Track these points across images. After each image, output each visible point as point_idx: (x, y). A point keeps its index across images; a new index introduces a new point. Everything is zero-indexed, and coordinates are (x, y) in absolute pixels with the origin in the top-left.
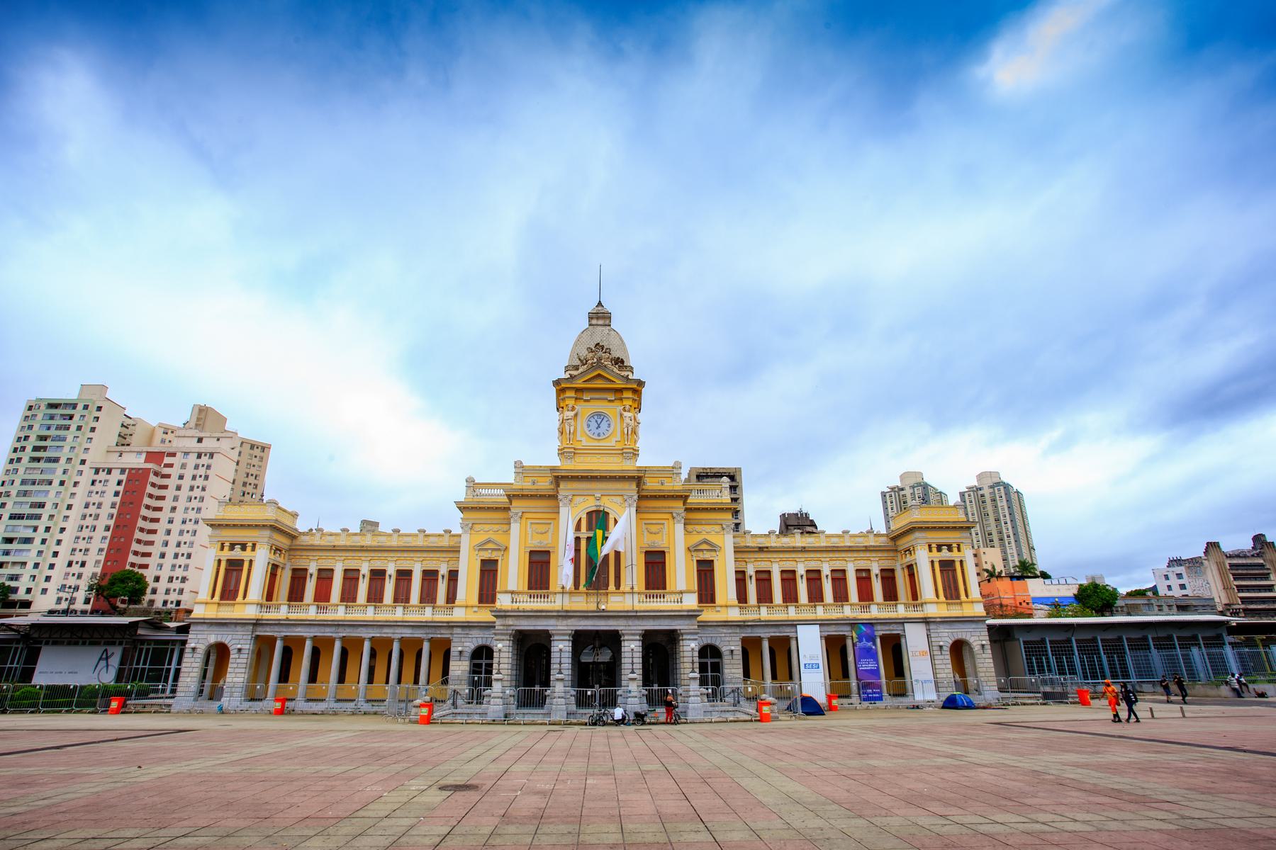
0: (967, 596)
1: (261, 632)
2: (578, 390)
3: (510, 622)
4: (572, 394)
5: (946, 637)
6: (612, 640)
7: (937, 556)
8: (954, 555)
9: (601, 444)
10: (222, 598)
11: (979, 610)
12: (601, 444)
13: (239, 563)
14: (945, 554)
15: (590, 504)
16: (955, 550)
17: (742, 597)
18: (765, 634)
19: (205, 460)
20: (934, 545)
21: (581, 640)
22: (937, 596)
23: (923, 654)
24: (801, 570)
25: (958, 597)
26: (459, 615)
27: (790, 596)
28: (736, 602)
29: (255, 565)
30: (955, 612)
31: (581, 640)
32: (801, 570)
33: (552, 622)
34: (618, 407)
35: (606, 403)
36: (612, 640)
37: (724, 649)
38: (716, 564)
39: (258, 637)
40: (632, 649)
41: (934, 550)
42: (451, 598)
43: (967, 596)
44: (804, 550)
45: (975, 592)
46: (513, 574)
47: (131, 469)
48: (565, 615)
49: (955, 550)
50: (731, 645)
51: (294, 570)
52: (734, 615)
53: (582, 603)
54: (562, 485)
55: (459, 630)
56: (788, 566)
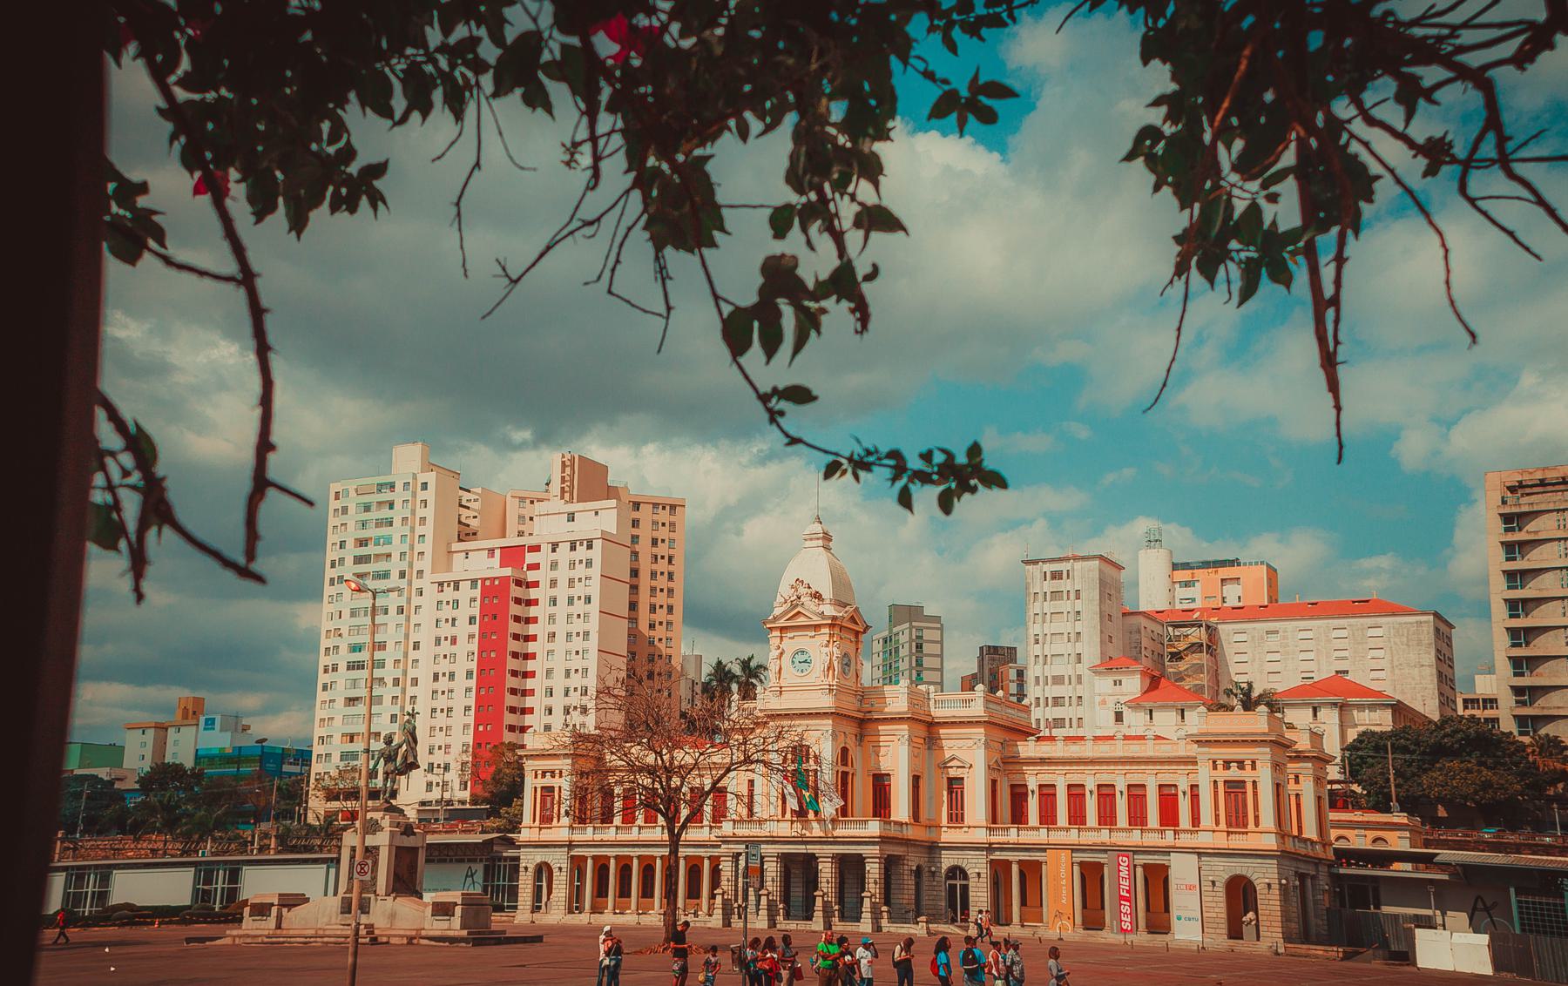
0: (1257, 824)
2: (782, 629)
5: (1223, 870)
7: (1222, 775)
8: (1247, 775)
9: (804, 680)
11: (1270, 842)
12: (804, 680)
13: (551, 789)
14: (1234, 773)
16: (1248, 768)
19: (581, 553)
20: (1220, 762)
21: (786, 860)
22: (1217, 823)
23: (1191, 888)
24: (1090, 785)
30: (1238, 842)
31: (786, 860)
32: (1090, 785)
37: (971, 872)
41: (1220, 767)
43: (1257, 824)
44: (1093, 762)
47: (484, 580)
50: (977, 865)
52: (981, 836)
53: (784, 829)
56: (1075, 779)
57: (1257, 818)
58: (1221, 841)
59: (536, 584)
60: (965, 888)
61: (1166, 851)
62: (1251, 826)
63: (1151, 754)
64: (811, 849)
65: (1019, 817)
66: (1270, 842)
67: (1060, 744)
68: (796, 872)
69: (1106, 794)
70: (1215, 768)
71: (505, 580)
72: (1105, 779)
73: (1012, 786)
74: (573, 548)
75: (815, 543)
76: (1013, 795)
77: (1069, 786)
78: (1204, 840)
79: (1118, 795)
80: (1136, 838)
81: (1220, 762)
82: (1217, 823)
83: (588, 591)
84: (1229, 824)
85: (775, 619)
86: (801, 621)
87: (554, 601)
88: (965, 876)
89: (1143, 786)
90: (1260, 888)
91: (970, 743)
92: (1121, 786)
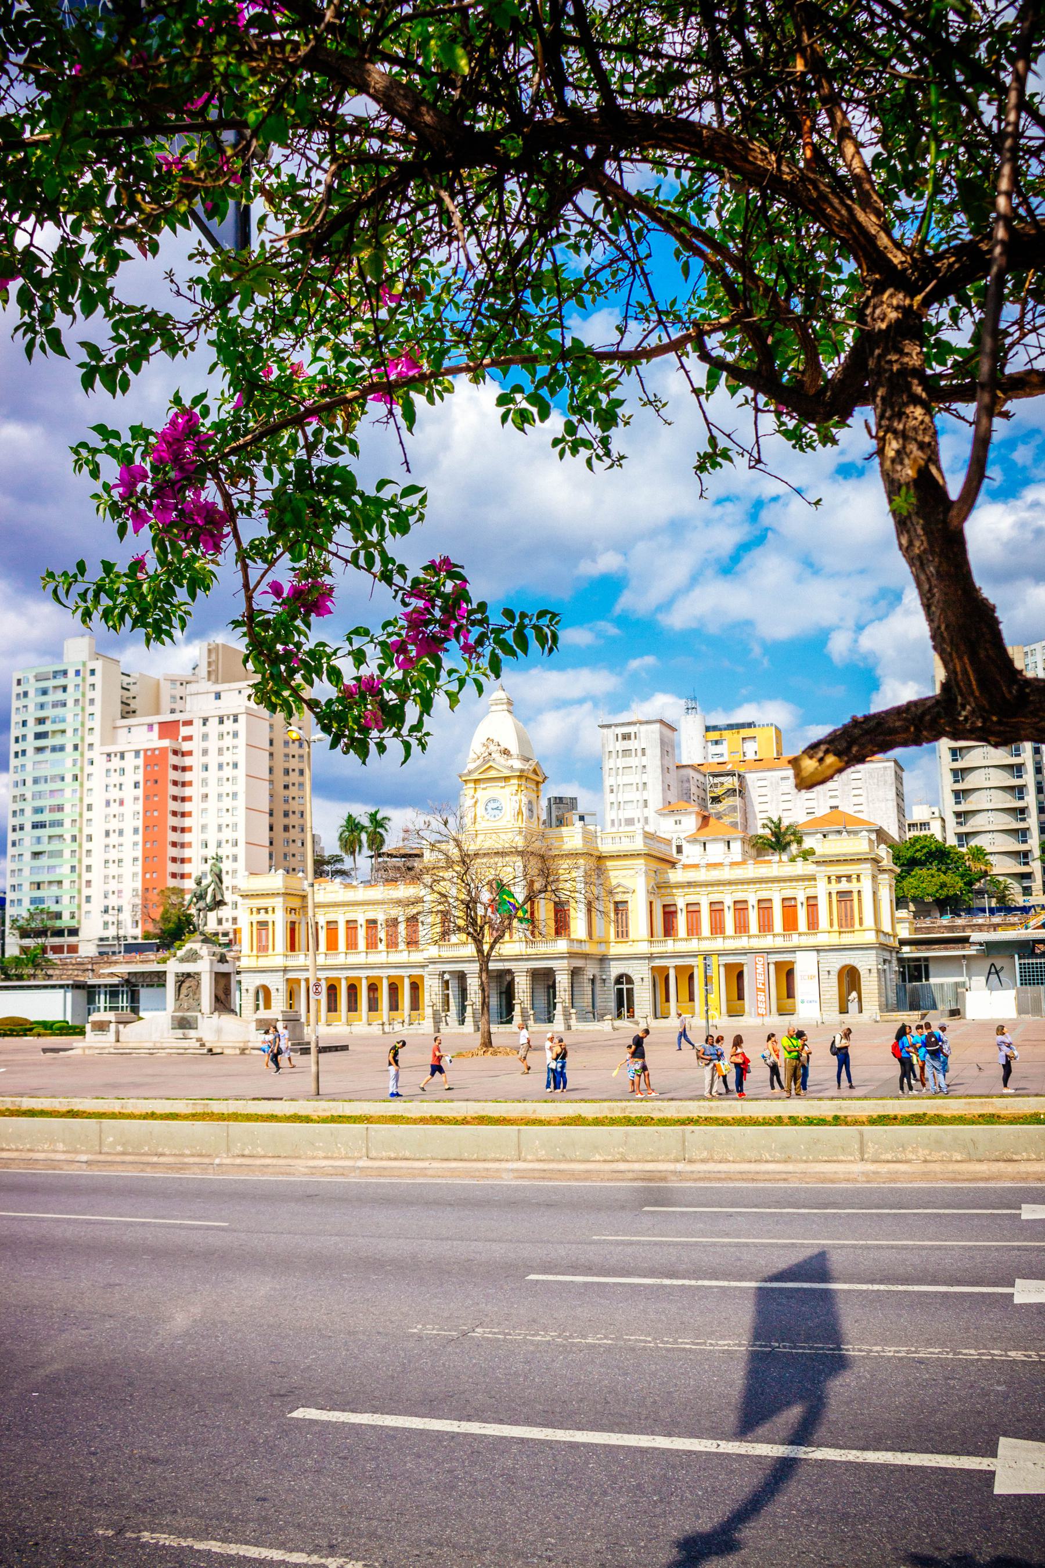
0: (861, 924)
2: (476, 781)
4: (471, 785)
5: (837, 961)
10: (259, 949)
11: (870, 937)
13: (266, 923)
14: (844, 886)
18: (670, 963)
19: (229, 725)
22: (832, 925)
23: (811, 977)
24: (728, 901)
30: (847, 939)
37: (636, 978)
38: (630, 906)
39: (287, 980)
43: (861, 924)
44: (730, 883)
47: (146, 750)
50: (641, 974)
52: (644, 948)
57: (861, 919)
58: (834, 939)
59: (190, 753)
60: (630, 991)
61: (793, 951)
62: (857, 926)
63: (800, 872)
64: (507, 965)
65: (669, 930)
66: (870, 937)
67: (703, 870)
68: (453, 984)
69: (765, 906)
70: (830, 882)
71: (164, 750)
72: (740, 896)
73: (664, 906)
74: (221, 722)
76: (665, 913)
77: (664, 906)
78: (822, 939)
79: (799, 905)
80: (767, 942)
82: (832, 925)
83: (235, 758)
84: (840, 926)
85: (470, 772)
86: (492, 774)
87: (206, 768)
88: (630, 981)
89: (746, 901)
90: (863, 973)
91: (632, 872)
92: (752, 901)
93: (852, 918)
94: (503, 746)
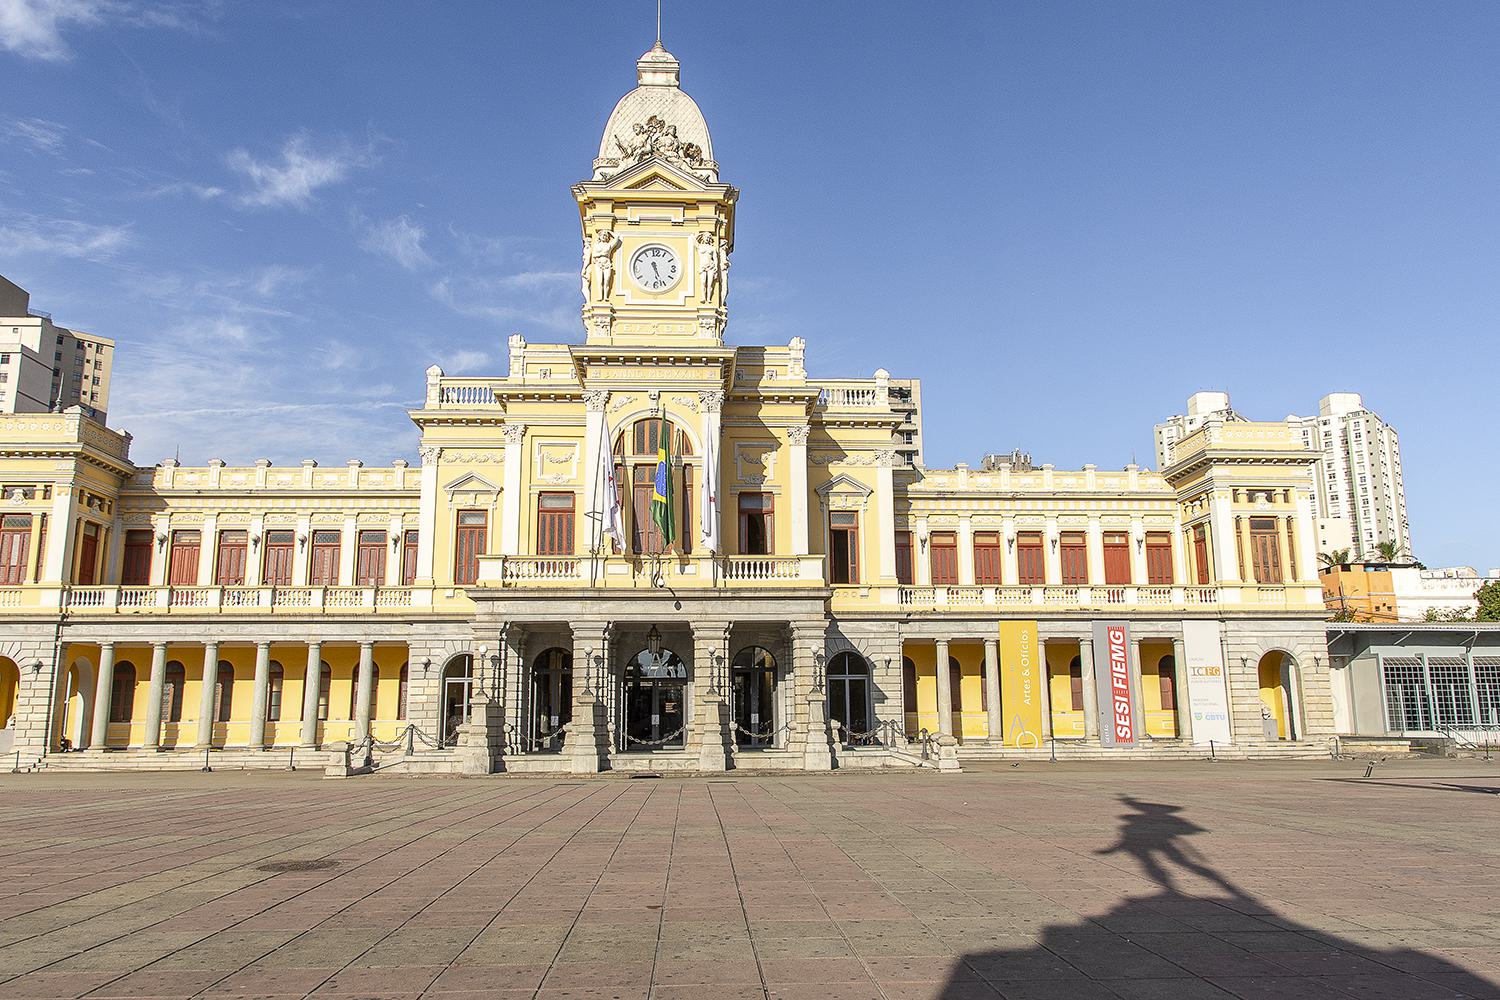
0: (1295, 578)
1: (71, 634)
2: (619, 204)
3: (501, 607)
4: (604, 209)
5: (1256, 642)
6: (677, 640)
7: (1247, 510)
8: (1278, 508)
11: (1314, 600)
14: (1261, 507)
15: (643, 406)
16: (1280, 498)
17: (905, 573)
20: (1242, 490)
21: (625, 639)
22: (1243, 577)
23: (1212, 671)
25: (1279, 580)
26: (420, 601)
27: (988, 573)
28: (895, 581)
29: (52, 523)
30: (1272, 600)
33: (575, 606)
34: (692, 231)
35: (668, 228)
36: (677, 640)
40: (710, 649)
41: (1243, 498)
42: (408, 576)
43: (1295, 578)
45: (1309, 569)
46: (511, 531)
48: (600, 596)
49: (1280, 498)
50: (882, 651)
51: (130, 533)
54: (591, 371)
55: (422, 628)
75: (661, 78)
81: (1242, 490)
85: (608, 181)
86: (656, 191)
93: (1277, 564)
94: (684, 138)
